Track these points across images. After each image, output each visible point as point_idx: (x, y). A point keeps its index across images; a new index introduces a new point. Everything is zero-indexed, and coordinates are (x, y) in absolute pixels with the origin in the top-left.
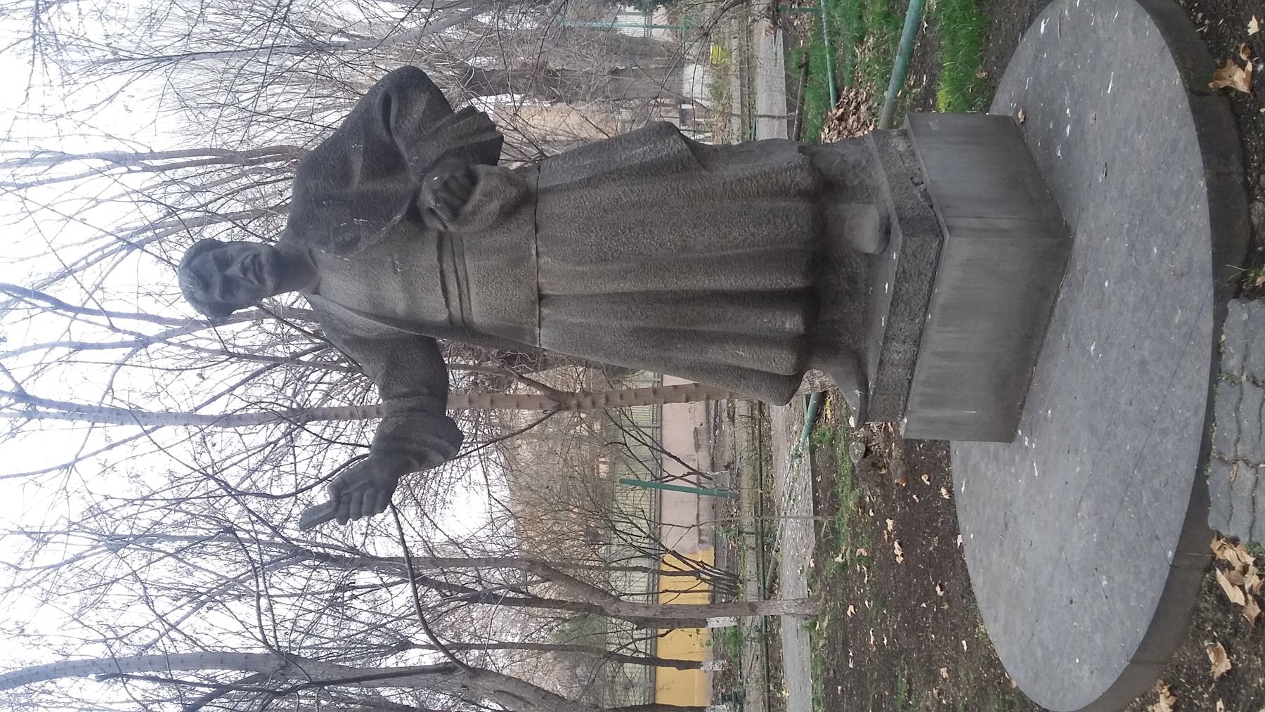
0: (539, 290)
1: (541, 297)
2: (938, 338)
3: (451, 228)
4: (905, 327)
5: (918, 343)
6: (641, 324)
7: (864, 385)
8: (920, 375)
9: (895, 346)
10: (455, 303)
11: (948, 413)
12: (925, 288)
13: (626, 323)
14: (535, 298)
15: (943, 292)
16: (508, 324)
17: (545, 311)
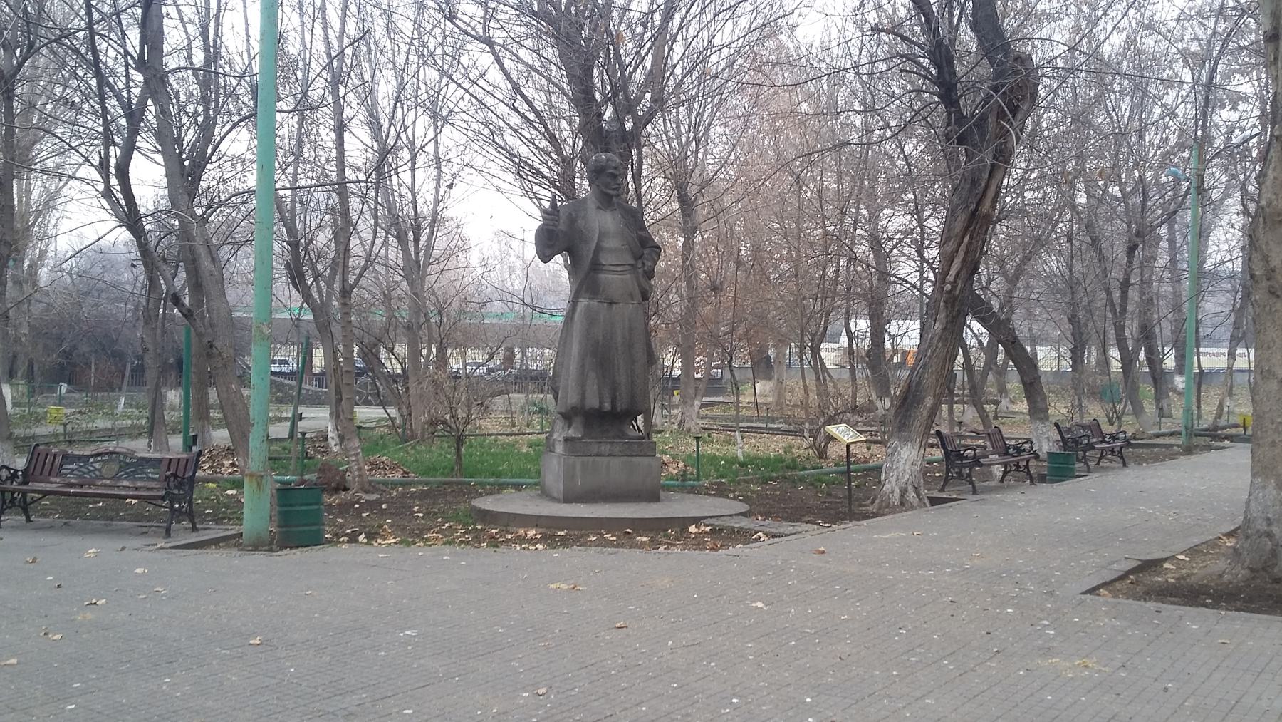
0: (616, 303)
1: (611, 303)
2: (616, 462)
3: (640, 271)
4: (617, 449)
5: (609, 455)
6: (600, 343)
7: (582, 438)
8: (597, 459)
9: (608, 447)
10: (612, 268)
11: (578, 473)
12: (634, 454)
13: (601, 338)
14: (615, 301)
15: (635, 459)
16: (601, 289)
17: (605, 305)
